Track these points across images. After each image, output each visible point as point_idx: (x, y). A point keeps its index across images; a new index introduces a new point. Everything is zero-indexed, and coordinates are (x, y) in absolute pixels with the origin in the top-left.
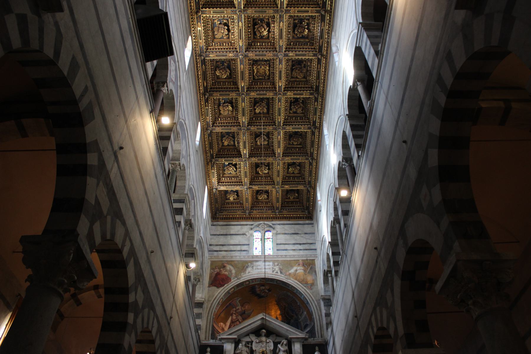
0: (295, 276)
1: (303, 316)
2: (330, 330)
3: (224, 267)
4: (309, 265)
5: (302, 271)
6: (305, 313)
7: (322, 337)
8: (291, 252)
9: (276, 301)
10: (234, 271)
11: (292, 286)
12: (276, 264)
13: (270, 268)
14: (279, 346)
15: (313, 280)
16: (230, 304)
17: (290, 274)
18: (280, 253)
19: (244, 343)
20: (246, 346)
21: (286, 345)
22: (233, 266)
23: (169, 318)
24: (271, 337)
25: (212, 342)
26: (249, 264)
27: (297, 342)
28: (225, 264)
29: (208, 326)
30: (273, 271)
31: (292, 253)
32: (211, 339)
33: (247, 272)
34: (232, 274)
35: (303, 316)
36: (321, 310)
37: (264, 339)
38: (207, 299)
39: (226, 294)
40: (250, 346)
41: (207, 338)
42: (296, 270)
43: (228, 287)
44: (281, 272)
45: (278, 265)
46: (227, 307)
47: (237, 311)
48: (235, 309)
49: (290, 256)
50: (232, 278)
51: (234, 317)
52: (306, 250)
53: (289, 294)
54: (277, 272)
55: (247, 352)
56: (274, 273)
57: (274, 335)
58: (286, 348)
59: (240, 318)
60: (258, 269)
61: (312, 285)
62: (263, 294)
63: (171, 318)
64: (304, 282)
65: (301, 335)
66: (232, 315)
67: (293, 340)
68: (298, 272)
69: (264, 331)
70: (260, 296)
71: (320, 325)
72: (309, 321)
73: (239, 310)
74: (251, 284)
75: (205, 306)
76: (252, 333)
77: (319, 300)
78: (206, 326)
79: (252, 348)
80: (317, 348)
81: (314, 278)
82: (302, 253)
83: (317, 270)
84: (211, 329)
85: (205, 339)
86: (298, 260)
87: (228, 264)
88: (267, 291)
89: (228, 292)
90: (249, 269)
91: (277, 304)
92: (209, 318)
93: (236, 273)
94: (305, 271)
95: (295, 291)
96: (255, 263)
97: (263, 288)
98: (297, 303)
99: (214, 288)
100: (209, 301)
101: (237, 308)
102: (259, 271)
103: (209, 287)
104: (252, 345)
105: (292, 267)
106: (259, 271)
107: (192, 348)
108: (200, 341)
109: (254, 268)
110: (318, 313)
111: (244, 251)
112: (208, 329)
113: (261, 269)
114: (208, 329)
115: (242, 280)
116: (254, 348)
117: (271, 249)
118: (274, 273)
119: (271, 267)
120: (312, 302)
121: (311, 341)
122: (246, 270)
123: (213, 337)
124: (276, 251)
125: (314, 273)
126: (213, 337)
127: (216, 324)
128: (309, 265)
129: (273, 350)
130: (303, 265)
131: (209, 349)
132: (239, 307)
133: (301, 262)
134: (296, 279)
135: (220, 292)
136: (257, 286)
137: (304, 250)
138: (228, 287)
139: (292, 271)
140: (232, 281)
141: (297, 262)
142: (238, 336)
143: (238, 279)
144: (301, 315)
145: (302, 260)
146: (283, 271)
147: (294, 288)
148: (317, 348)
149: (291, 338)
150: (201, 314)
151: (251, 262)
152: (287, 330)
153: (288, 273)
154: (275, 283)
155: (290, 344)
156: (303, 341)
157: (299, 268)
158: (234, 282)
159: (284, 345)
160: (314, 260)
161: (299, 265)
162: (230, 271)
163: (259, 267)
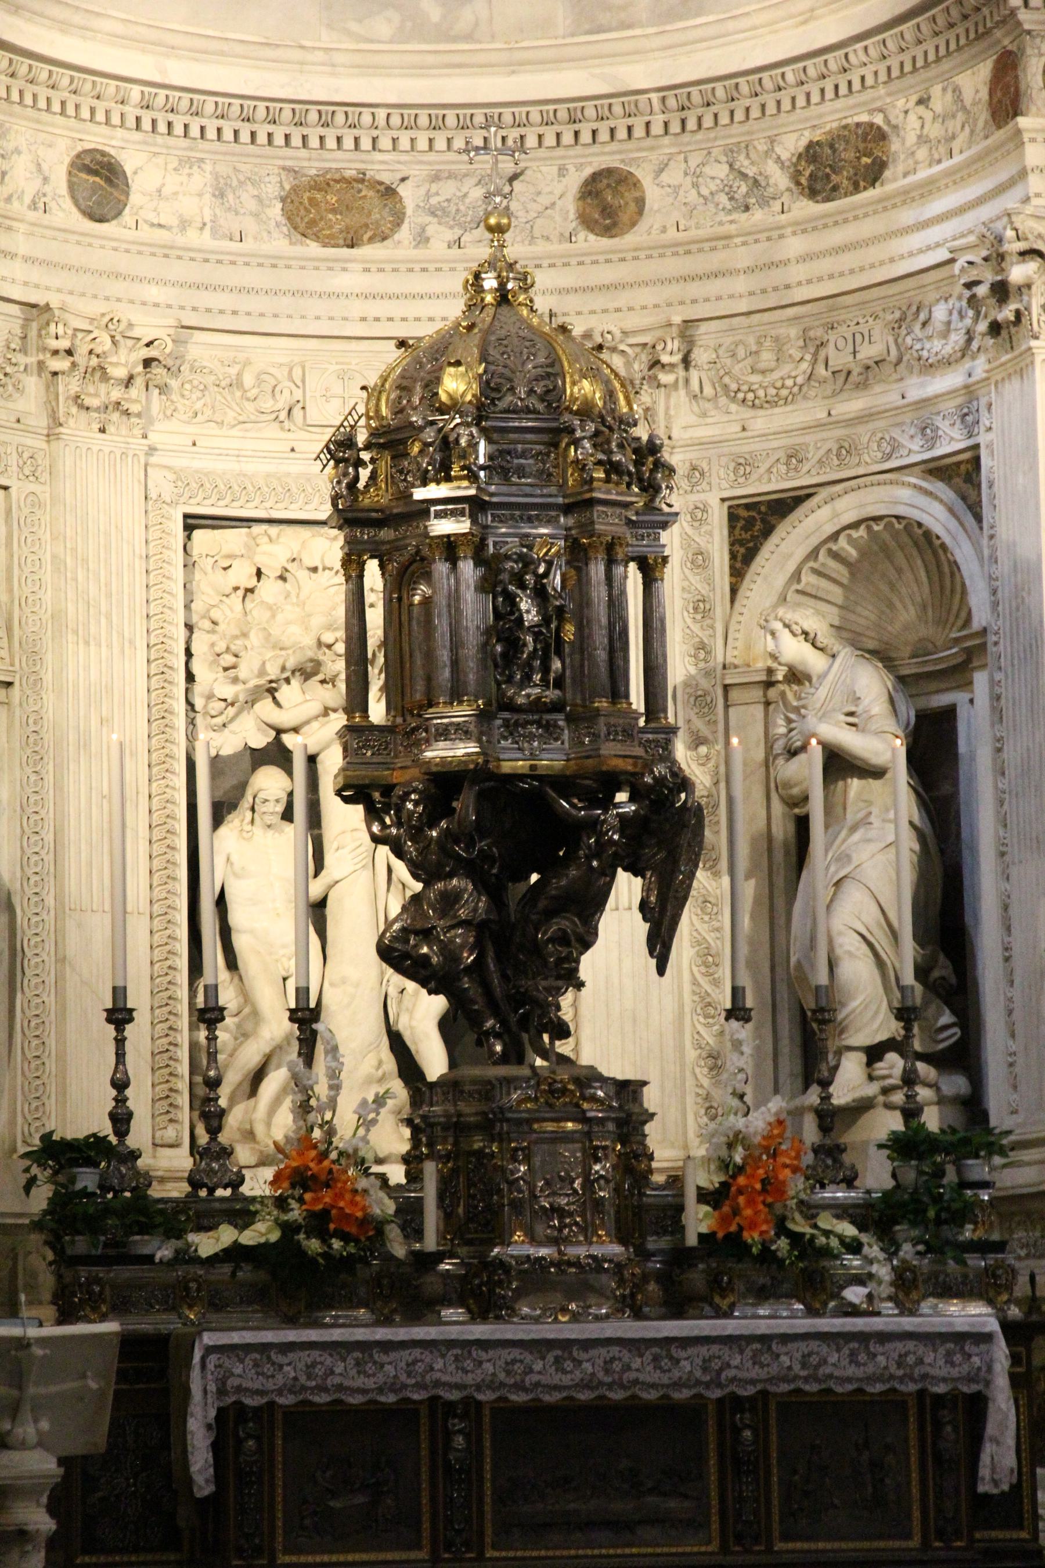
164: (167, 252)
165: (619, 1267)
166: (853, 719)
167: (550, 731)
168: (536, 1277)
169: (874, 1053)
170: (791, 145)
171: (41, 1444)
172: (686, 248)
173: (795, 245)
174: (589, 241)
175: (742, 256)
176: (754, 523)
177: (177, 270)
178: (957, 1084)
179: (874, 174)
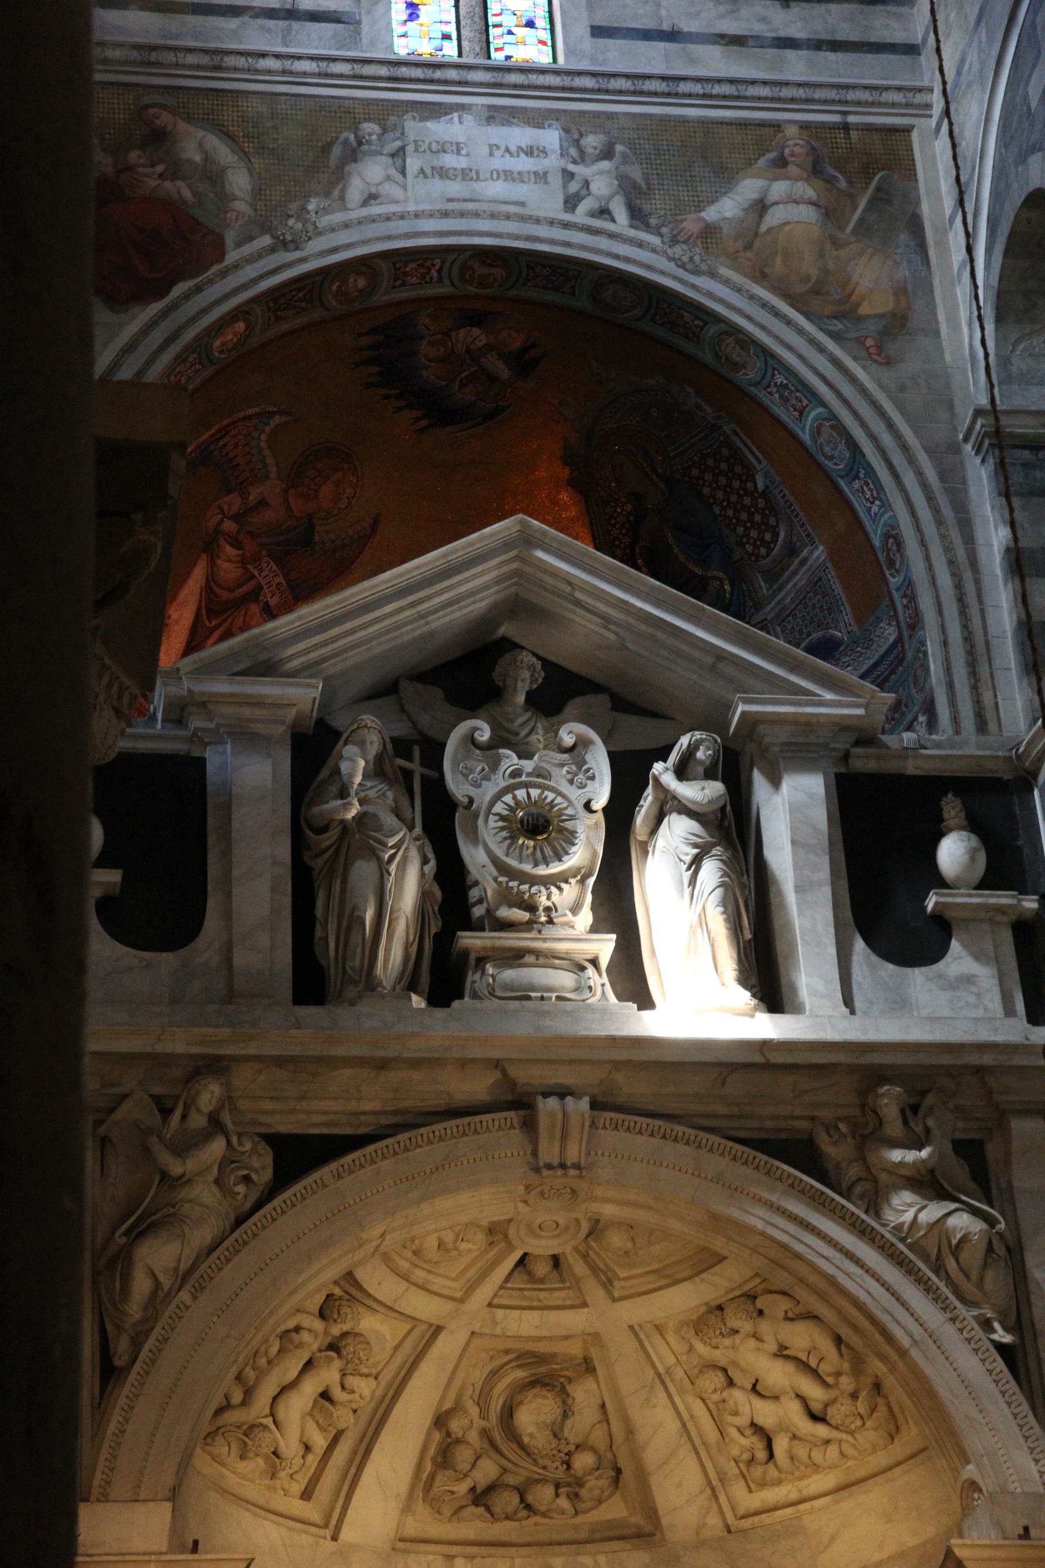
0: (752, 247)
1: (801, 579)
3: (157, 139)
4: (867, 171)
5: (807, 214)
7: (982, 727)
8: (714, 52)
10: (239, 181)
11: (734, 330)
12: (592, 142)
13: (541, 177)
15: (900, 291)
17: (709, 233)
18: (619, 56)
22: (229, 137)
26: (370, 128)
28: (165, 119)
30: (571, 203)
31: (715, 62)
33: (355, 189)
34: (225, 198)
36: (966, 525)
40: (415, 767)
42: (761, 207)
44: (637, 216)
45: (607, 154)
48: (234, 502)
49: (710, 91)
50: (230, 237)
51: (228, 569)
52: (836, 46)
54: (604, 212)
56: (580, 216)
57: (600, 702)
59: (269, 576)
60: (443, 173)
61: (894, 331)
64: (824, 300)
66: (210, 546)
68: (775, 217)
70: (440, 411)
71: (968, 638)
72: (847, 615)
73: (269, 515)
74: (381, 298)
77: (955, 449)
80: (952, 808)
81: (903, 272)
82: (796, 66)
83: (925, 208)
86: (776, 126)
87: (189, 119)
88: (503, 371)
89: (200, 346)
90: (372, 172)
91: (574, 483)
93: (257, 193)
94: (831, 213)
96: (412, 127)
97: (477, 336)
98: (750, 474)
101: (254, 494)
102: (455, 188)
105: (726, 176)
106: (455, 188)
109: (413, 163)
110: (948, 549)
111: (316, 17)
113: (465, 175)
115: (317, 254)
117: (542, 23)
118: (580, 216)
119: (552, 162)
120: (898, 460)
122: (340, 176)
124: (588, 44)
125: (903, 237)
128: (865, 171)
130: (816, 170)
133: (795, 143)
134: (761, 276)
137: (818, 45)
139: (727, 208)
140: (232, 256)
141: (758, 144)
143: (282, 244)
144: (773, 576)
145: (805, 126)
146: (657, 205)
147: (746, 341)
151: (386, 114)
152: (721, 656)
153: (690, 225)
156: (841, 744)
157: (779, 189)
158: (252, 268)
160: (908, 130)
161: (781, 162)
162: (213, 176)
163: (449, 160)
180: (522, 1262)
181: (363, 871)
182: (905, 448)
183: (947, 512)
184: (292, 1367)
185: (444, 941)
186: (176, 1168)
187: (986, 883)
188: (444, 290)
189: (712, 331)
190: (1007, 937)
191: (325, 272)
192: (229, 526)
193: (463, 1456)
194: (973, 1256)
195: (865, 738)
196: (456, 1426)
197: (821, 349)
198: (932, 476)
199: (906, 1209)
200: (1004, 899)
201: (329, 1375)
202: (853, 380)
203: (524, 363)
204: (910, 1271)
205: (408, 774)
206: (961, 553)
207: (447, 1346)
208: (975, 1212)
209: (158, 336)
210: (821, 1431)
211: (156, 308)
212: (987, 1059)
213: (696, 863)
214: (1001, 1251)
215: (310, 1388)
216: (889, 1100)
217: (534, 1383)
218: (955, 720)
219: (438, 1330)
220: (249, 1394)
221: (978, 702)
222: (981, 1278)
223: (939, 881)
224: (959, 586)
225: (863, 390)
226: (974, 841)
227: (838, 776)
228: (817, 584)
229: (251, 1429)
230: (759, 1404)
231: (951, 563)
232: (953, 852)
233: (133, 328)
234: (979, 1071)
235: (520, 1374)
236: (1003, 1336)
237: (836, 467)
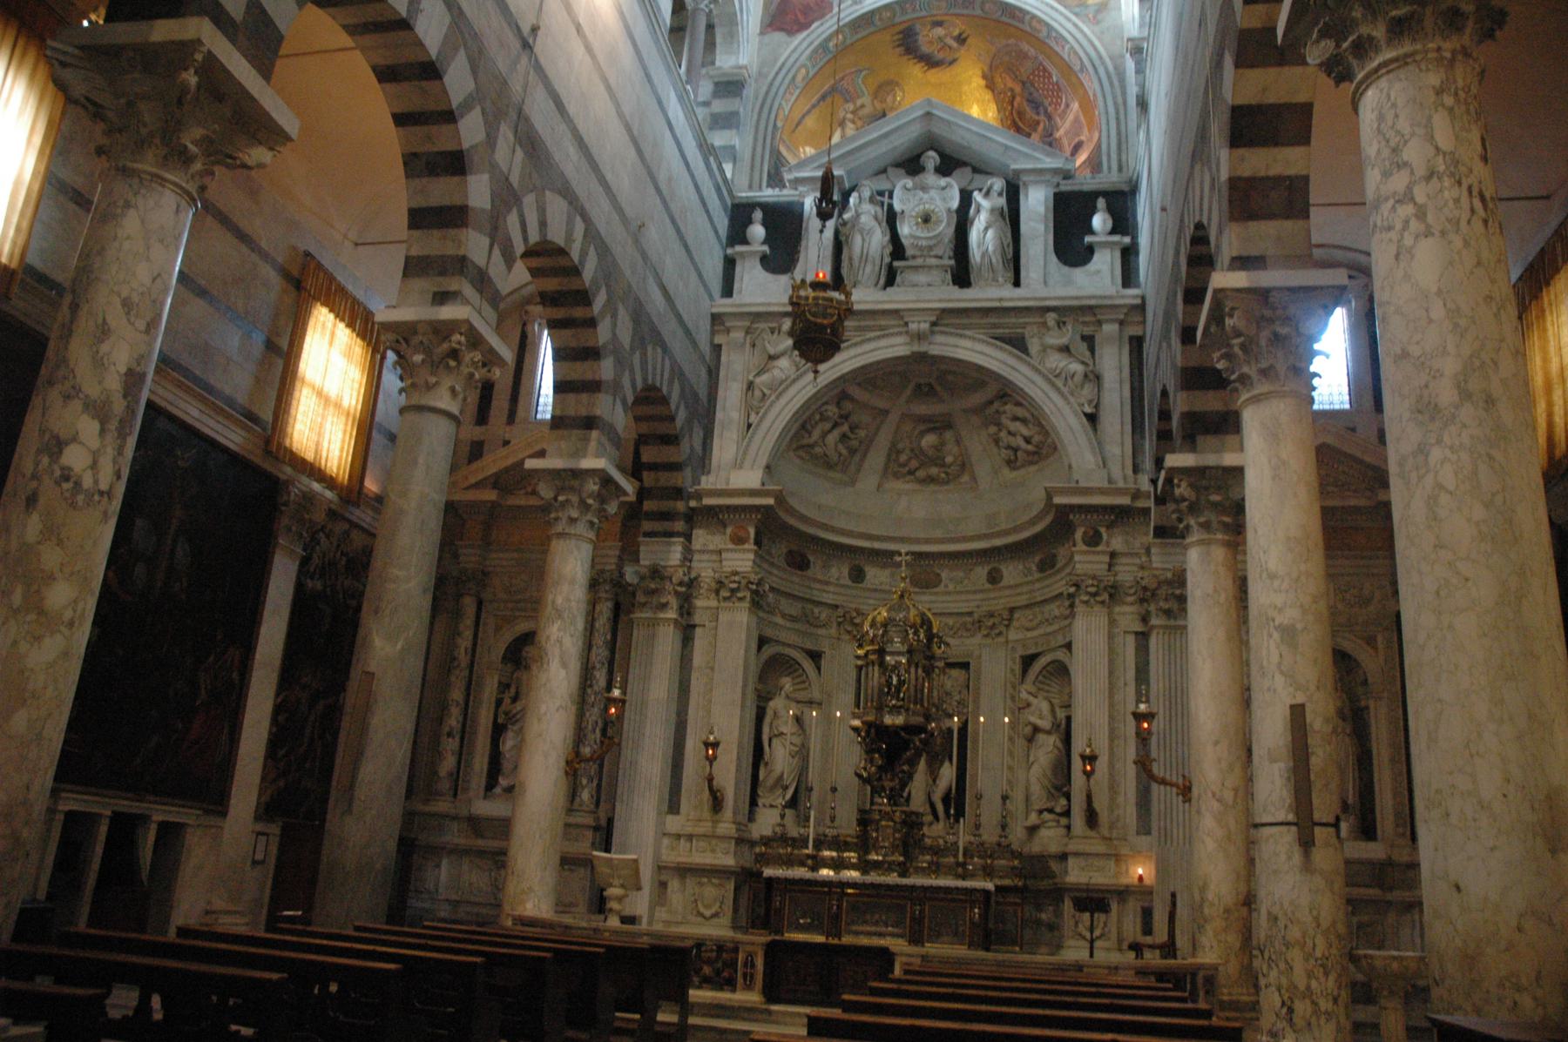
1: (1071, 117)
2: (1142, 135)
6: (1075, 106)
7: (1120, 169)
9: (984, 77)
11: (1034, 17)
14: (977, 196)
16: (833, 89)
19: (867, 194)
20: (872, 200)
21: (1000, 194)
23: (526, 29)
24: (957, 173)
25: (769, 194)
27: (1036, 182)
29: (759, 149)
32: (769, 185)
35: (1071, 117)
37: (930, 178)
38: (754, 70)
39: (815, 51)
40: (886, 200)
41: (755, 185)
43: (822, 29)
46: (823, 98)
47: (860, 113)
48: (851, 107)
53: (1025, 47)
55: (876, 218)
57: (969, 169)
58: (1002, 201)
62: (940, 56)
63: (535, 30)
65: (1049, 162)
66: (842, 124)
67: (1025, 178)
69: (932, 153)
70: (931, 62)
71: (1119, 134)
74: (898, 20)
75: (749, 92)
76: (898, 165)
77: (1123, 56)
78: (754, 149)
79: (891, 206)
80: (1101, 203)
84: (767, 157)
85: (750, 187)
88: (955, 45)
89: (824, 46)
91: (987, 87)
92: (762, 127)
95: (1044, 34)
97: (940, 31)
98: (1050, 76)
99: (779, 37)
100: (760, 73)
101: (859, 102)
103: (762, 33)
104: (891, 197)
107: (685, 191)
108: (730, 192)
110: (1114, 98)
112: (758, 159)
114: (758, 159)
116: (897, 207)
121: (1086, 181)
123: (775, 179)
126: (775, 179)
127: (788, 148)
129: (958, 211)
131: (758, 215)
132: (866, 100)
135: (798, 47)
136: (918, 27)
138: (822, 29)
142: (849, 173)
144: (1063, 116)
147: (1040, 21)
148: (1101, 203)
149: (1018, 173)
150: (735, 114)
152: (1007, 147)
154: (978, 12)
155: (1013, 193)
156: (1056, 180)
159: (994, 194)
164: (876, 590)
165: (899, 864)
166: (1041, 718)
167: (899, 713)
168: (876, 866)
169: (1041, 812)
170: (1037, 559)
171: (622, 886)
172: (1010, 587)
173: (1037, 585)
174: (988, 586)
175: (1025, 589)
176: (1028, 661)
177: (878, 595)
178: (1064, 821)
179: (1053, 566)
180: (919, 386)
181: (857, 241)
182: (1101, 58)
183: (1116, 83)
184: (828, 426)
185: (890, 266)
186: (772, 351)
187: (1113, 232)
188: (924, 13)
189: (1027, 18)
190: (1118, 254)
191: (872, 13)
192: (849, 116)
193: (903, 458)
194: (1079, 378)
195: (1067, 175)
196: (900, 446)
197: (1069, 20)
198: (1111, 68)
199: (1056, 361)
200: (1116, 238)
201: (845, 428)
202: (1082, 31)
203: (961, 40)
204: (1053, 385)
205: (882, 204)
206: (1120, 100)
207: (893, 418)
208: (1083, 363)
209: (805, 44)
210: (1030, 447)
211: (805, 34)
212: (1093, 302)
213: (986, 229)
214: (1091, 376)
215: (836, 434)
216: (1051, 318)
217: (929, 430)
218: (1109, 168)
219: (886, 412)
220: (810, 433)
221: (1120, 161)
222: (1082, 387)
223: (1091, 232)
224: (1117, 113)
225: (1085, 35)
226: (1107, 216)
227: (1056, 195)
228: (1076, 120)
229: (811, 446)
230: (1011, 439)
231: (1115, 104)
232: (1099, 221)
233: (796, 42)
234: (1090, 308)
235: (922, 427)
236: (1088, 410)
237: (1077, 68)
